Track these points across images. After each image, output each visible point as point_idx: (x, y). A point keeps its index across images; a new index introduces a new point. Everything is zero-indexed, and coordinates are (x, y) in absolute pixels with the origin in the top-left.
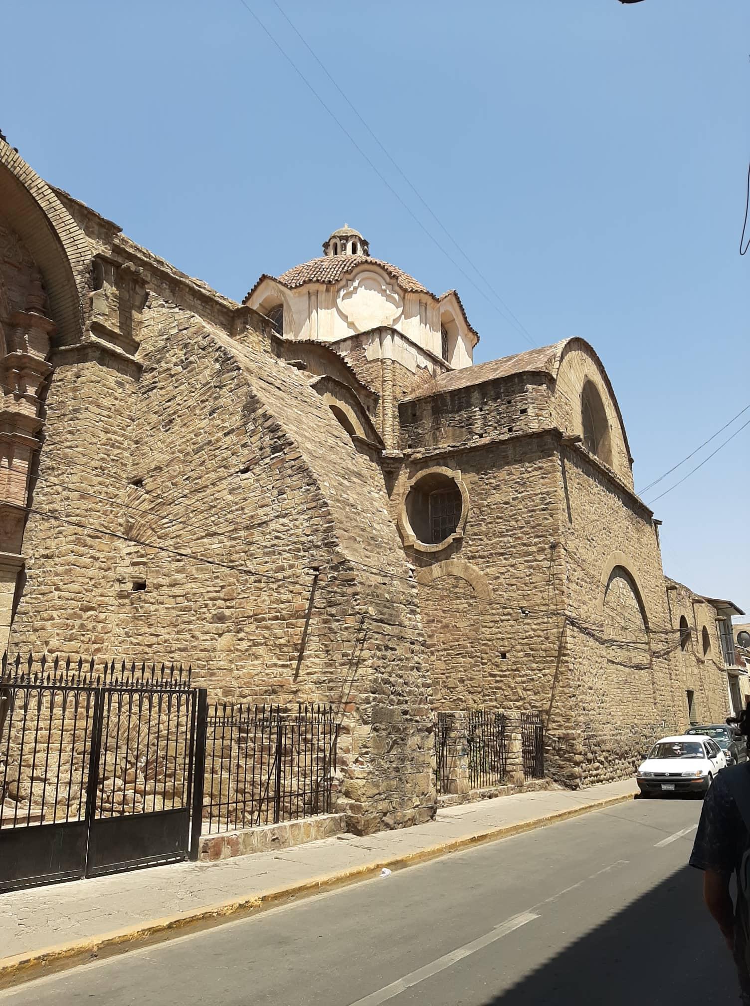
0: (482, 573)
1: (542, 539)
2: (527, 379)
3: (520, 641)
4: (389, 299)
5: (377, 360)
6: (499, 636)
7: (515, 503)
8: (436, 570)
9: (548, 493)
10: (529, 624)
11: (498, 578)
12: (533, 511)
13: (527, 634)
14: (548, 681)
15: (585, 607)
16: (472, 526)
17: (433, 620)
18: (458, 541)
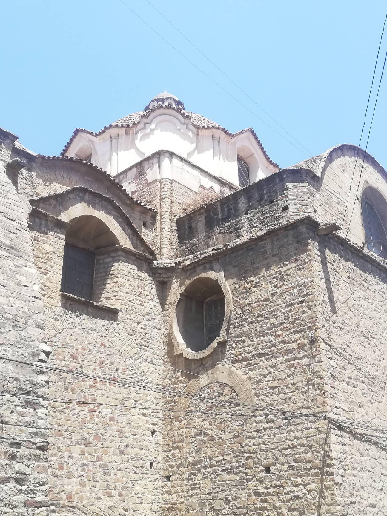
0: (245, 377)
1: (301, 334)
2: (287, 177)
3: (284, 451)
4: (184, 136)
5: (156, 180)
6: (263, 447)
7: (274, 299)
8: (204, 379)
9: (305, 285)
10: (291, 431)
11: (259, 381)
12: (292, 305)
13: (290, 443)
14: (314, 498)
15: (361, 410)
16: (235, 327)
17: (200, 434)
18: (222, 344)
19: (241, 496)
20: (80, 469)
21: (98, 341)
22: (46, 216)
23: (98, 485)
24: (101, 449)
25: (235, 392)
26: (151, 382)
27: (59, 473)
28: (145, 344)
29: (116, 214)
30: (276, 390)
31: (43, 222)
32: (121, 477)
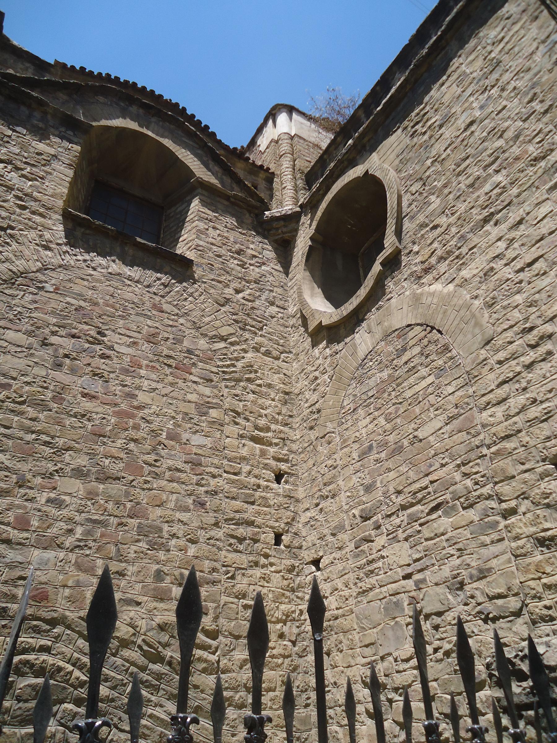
0: (451, 287)
19: (494, 563)
20: (79, 530)
21: (146, 298)
22: (41, 103)
23: (131, 569)
24: (142, 493)
25: (433, 328)
26: (269, 386)
27: (14, 534)
28: (254, 323)
29: (191, 143)
30: (540, 265)
31: (37, 114)
32: (197, 557)
